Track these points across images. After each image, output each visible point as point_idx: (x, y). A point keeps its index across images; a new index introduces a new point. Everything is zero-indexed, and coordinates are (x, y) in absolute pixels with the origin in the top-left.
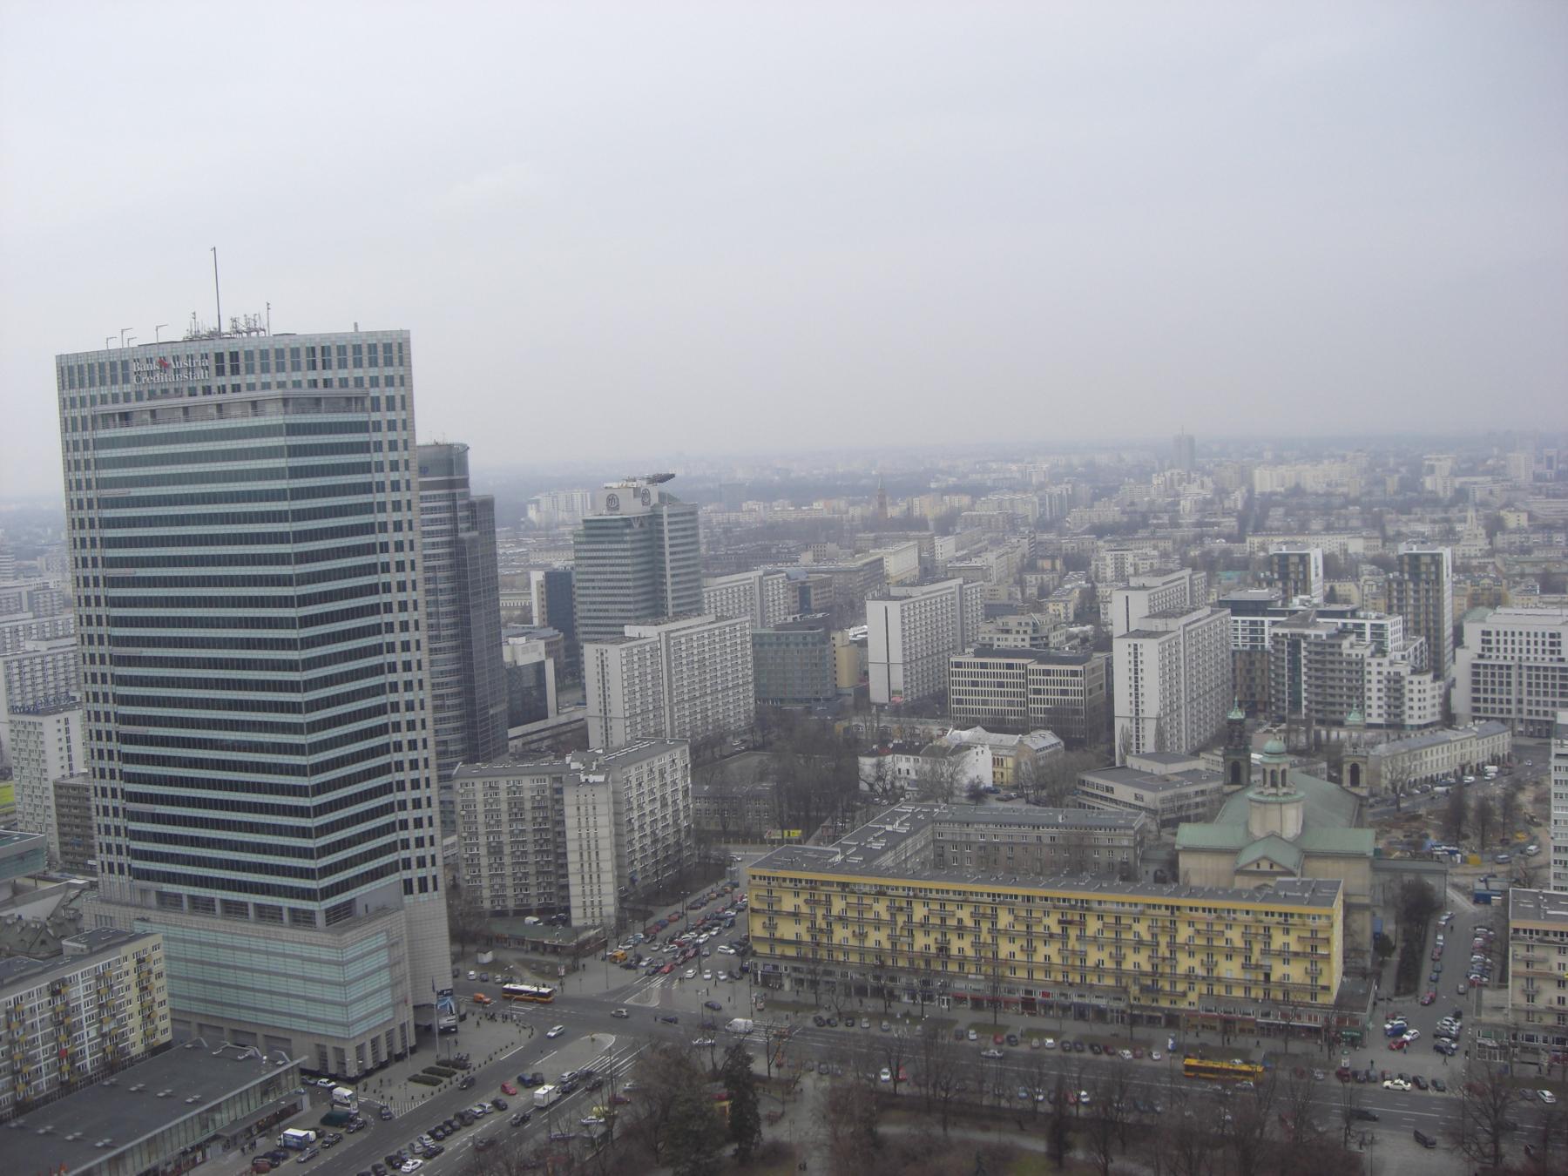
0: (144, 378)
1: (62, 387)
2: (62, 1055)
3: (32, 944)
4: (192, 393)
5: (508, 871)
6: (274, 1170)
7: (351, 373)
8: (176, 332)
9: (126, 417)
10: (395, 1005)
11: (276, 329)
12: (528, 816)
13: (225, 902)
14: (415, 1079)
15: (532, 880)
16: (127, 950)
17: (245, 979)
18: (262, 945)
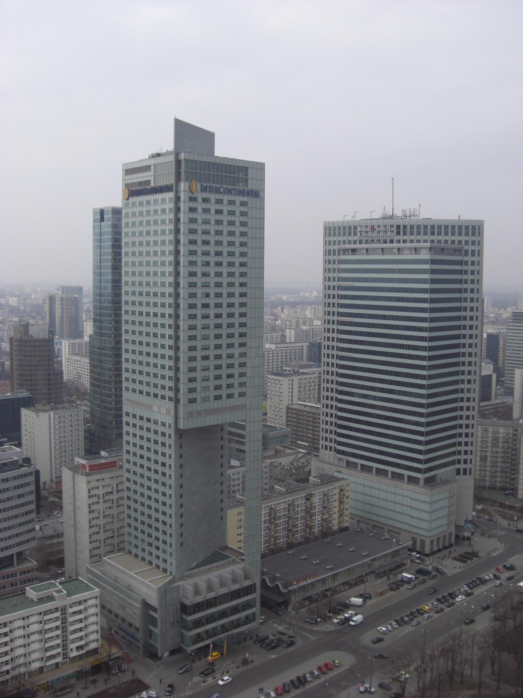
0: (364, 234)
1: (325, 236)
2: (307, 526)
3: (286, 475)
4: (385, 242)
5: (488, 469)
6: (397, 591)
7: (457, 238)
8: (377, 215)
9: (354, 251)
10: (448, 525)
11: (422, 217)
12: (501, 445)
13: (377, 469)
14: (455, 559)
15: (499, 474)
16: (337, 484)
17: (383, 504)
18: (393, 490)
